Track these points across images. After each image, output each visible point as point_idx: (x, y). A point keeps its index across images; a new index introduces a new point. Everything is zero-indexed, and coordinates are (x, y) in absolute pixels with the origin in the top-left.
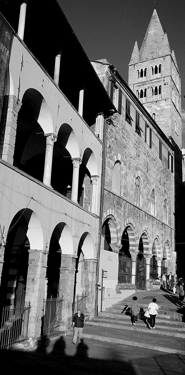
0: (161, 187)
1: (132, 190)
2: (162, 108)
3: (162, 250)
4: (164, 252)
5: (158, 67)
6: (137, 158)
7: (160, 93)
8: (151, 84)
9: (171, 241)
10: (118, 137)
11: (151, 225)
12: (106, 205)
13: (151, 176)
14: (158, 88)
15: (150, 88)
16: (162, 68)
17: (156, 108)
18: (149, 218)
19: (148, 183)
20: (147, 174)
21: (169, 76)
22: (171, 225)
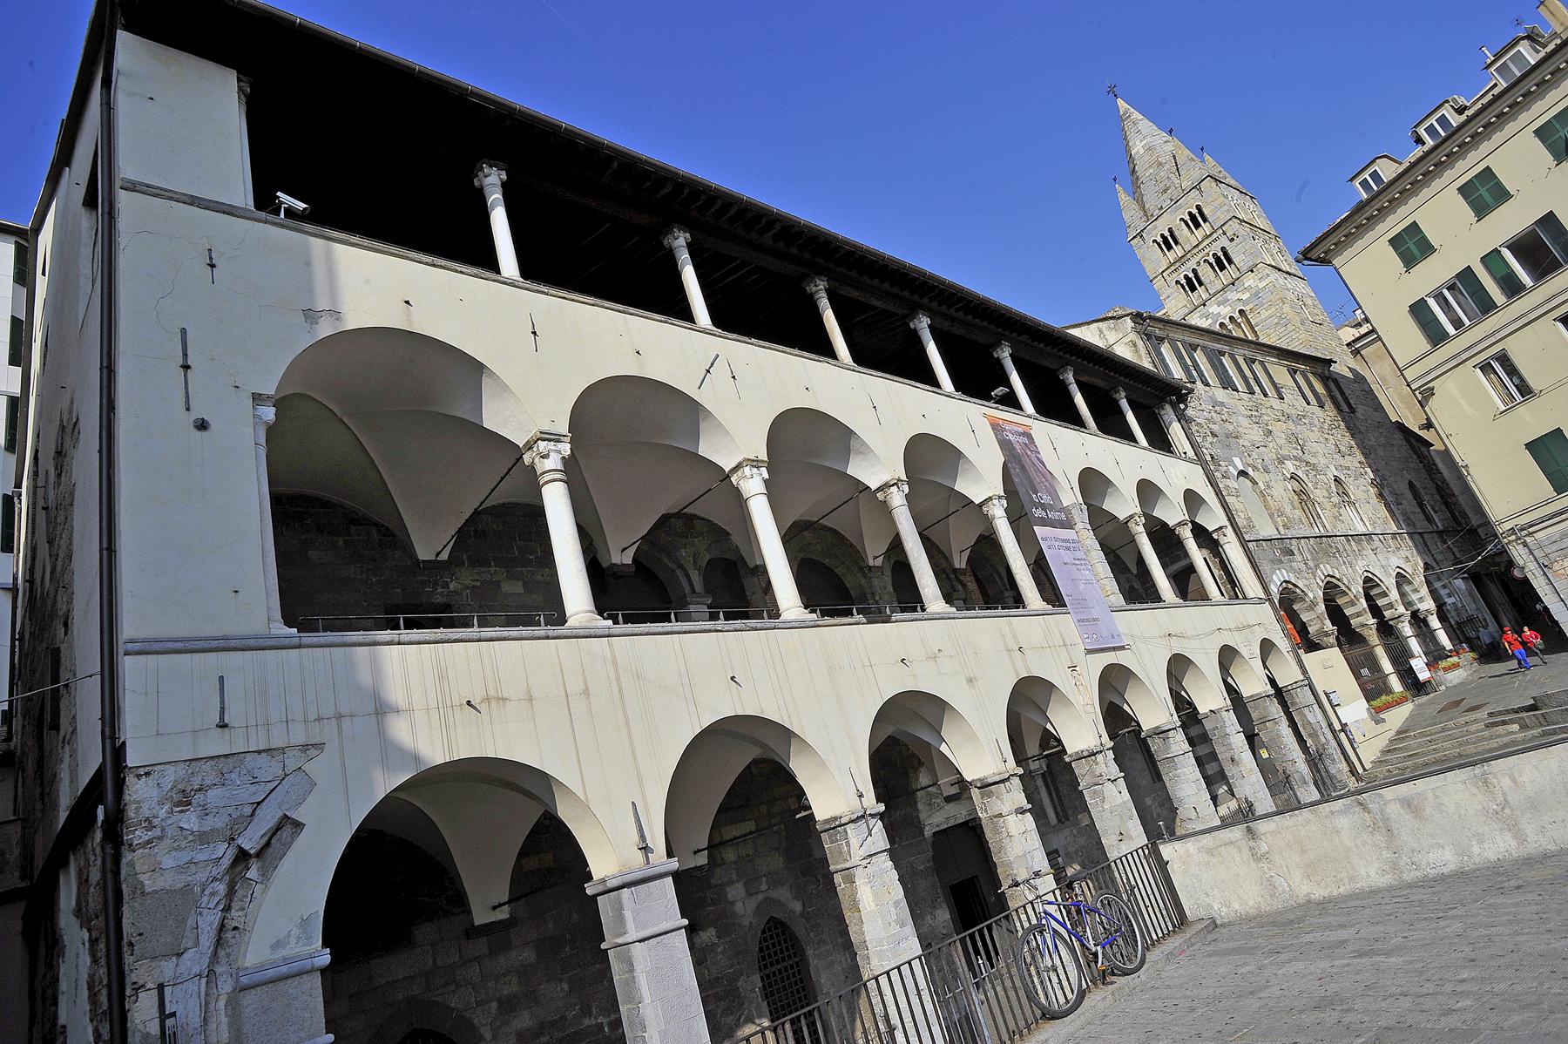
0: (1347, 461)
1: (1294, 508)
2: (1253, 291)
3: (1424, 591)
4: (1434, 593)
5: (1195, 211)
6: (1270, 438)
7: (1230, 262)
8: (1201, 255)
9: (1435, 560)
10: (1215, 428)
11: (1371, 552)
12: (1265, 568)
13: (1314, 455)
14: (1220, 254)
15: (1202, 262)
16: (1206, 212)
17: (1240, 296)
18: (1359, 543)
19: (1318, 472)
20: (1307, 457)
21: (1230, 219)
22: (1414, 526)
